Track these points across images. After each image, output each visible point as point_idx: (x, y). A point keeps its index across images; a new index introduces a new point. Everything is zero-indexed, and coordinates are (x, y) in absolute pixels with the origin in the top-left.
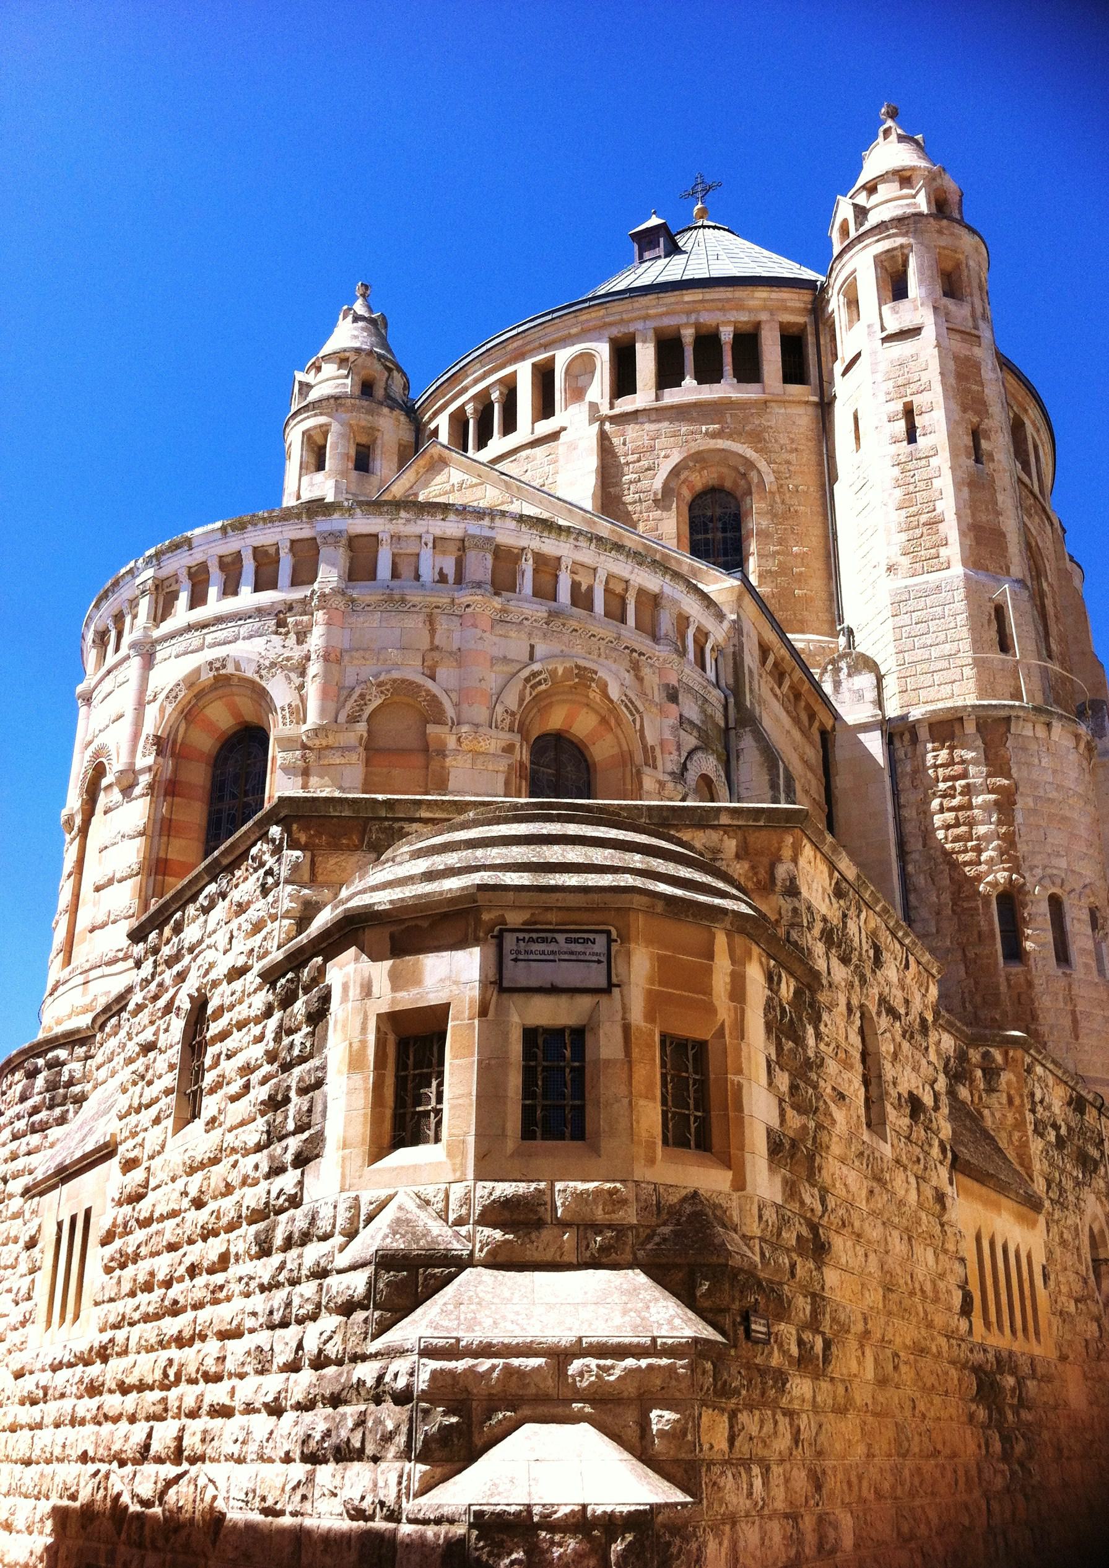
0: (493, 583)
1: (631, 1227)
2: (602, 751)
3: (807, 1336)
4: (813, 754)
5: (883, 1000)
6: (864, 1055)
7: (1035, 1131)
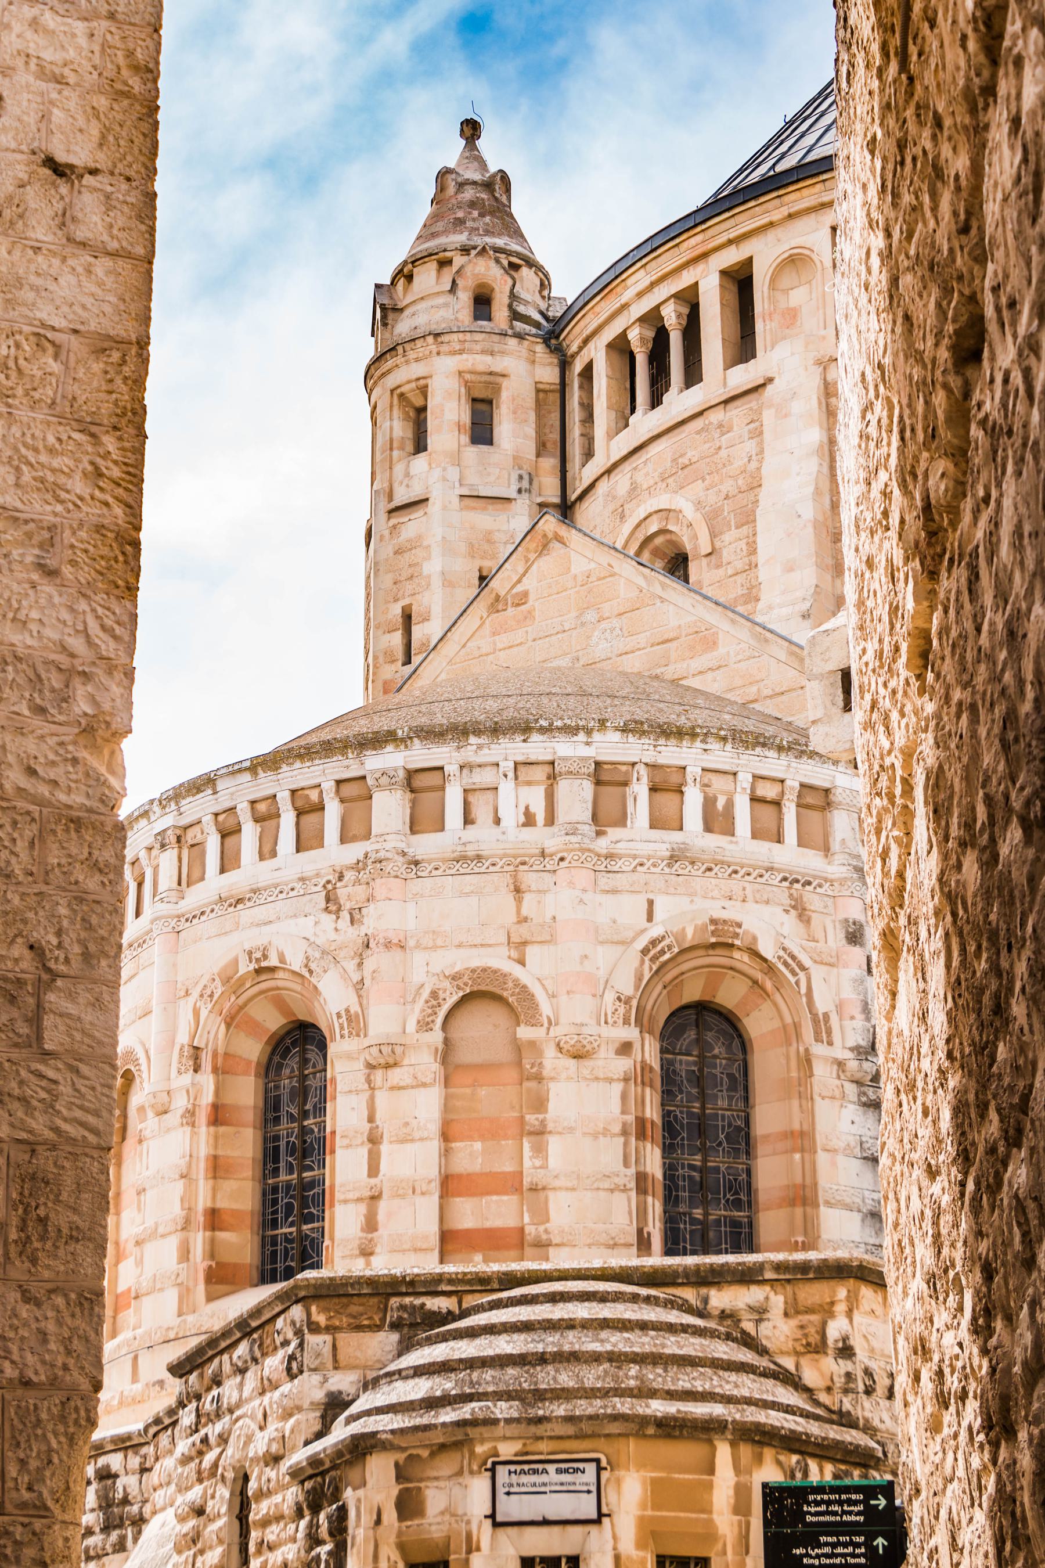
0: (595, 817)
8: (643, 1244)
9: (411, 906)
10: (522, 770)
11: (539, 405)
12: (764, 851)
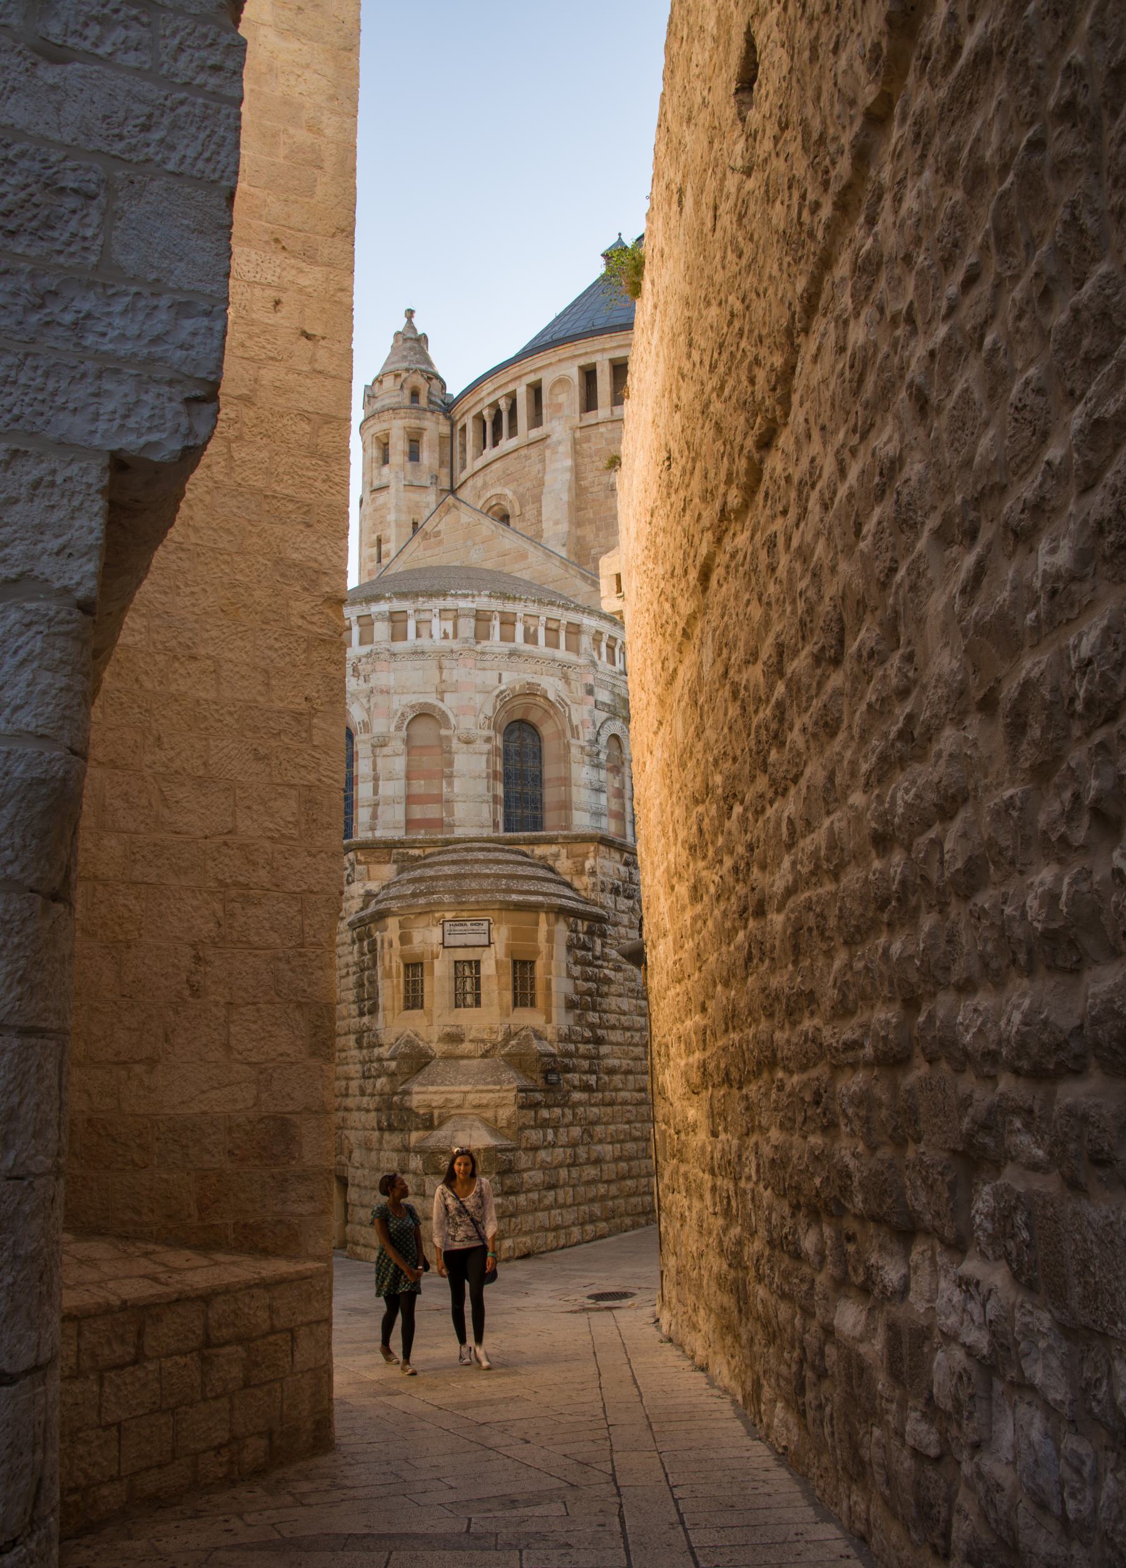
0: (476, 636)
2: (546, 730)
8: (496, 825)
9: (392, 675)
10: (443, 615)
11: (441, 444)
12: (549, 651)
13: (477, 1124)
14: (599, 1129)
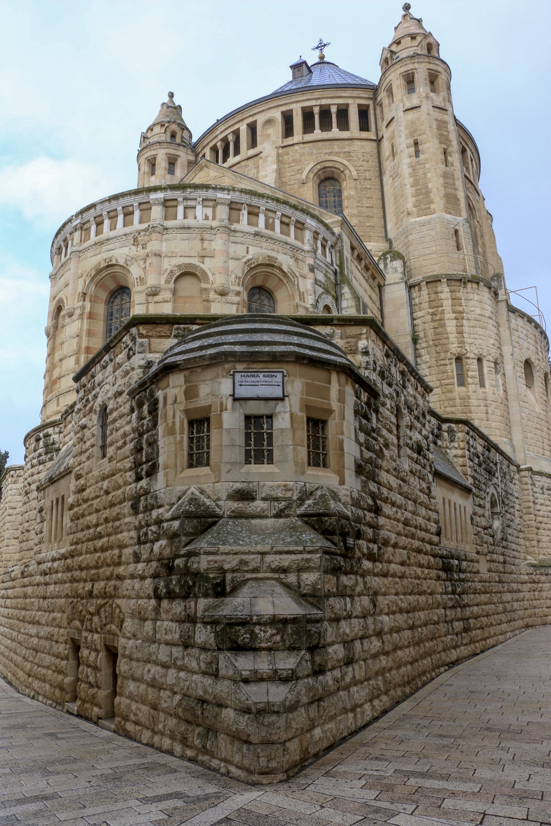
0: (229, 219)
1: (294, 501)
3: (371, 545)
4: (375, 297)
5: (406, 402)
6: (398, 427)
7: (470, 459)
9: (164, 244)
10: (206, 203)
12: (284, 238)
13: (279, 589)
14: (380, 598)
